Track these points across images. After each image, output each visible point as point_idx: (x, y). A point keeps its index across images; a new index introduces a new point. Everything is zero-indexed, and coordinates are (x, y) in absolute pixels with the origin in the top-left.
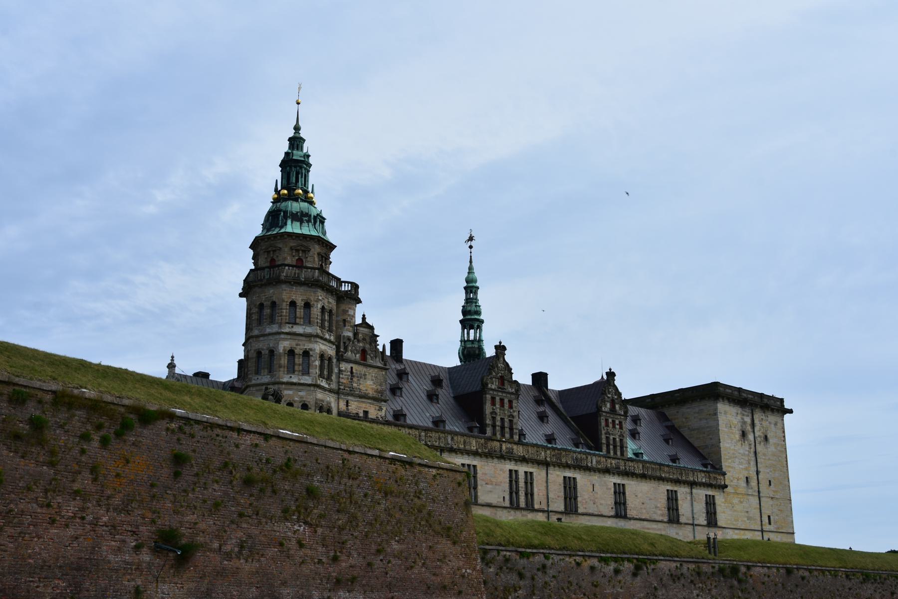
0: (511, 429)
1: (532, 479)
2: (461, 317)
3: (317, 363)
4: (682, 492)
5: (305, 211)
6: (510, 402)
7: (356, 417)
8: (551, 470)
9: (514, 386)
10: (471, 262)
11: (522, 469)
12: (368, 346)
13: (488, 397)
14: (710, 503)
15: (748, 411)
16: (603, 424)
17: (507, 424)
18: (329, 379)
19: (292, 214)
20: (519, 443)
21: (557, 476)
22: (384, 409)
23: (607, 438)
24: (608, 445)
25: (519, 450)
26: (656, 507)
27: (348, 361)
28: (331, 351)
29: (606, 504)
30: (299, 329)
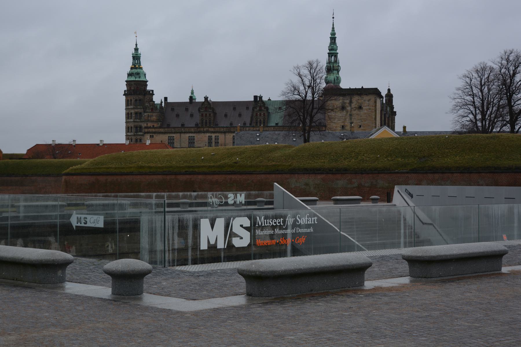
6: (210, 114)
7: (150, 128)
8: (227, 134)
10: (333, 25)
11: (213, 135)
18: (140, 119)
20: (213, 127)
23: (257, 120)
24: (257, 123)
25: (212, 130)
27: (147, 112)
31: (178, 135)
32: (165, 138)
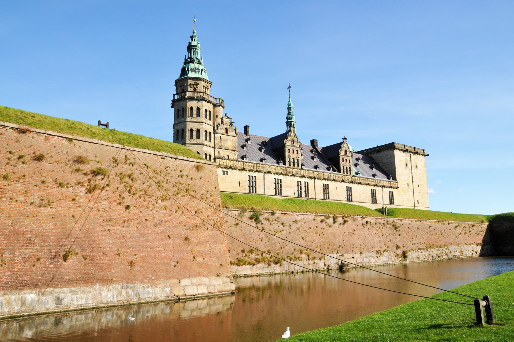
0: (298, 163)
1: (308, 185)
2: (286, 121)
3: (204, 134)
4: (378, 190)
5: (197, 67)
6: (297, 151)
7: (224, 158)
9: (299, 144)
11: (303, 180)
12: (228, 127)
13: (287, 149)
14: (391, 195)
15: (408, 154)
16: (341, 160)
17: (296, 161)
19: (191, 69)
21: (320, 183)
22: (237, 154)
24: (344, 170)
26: (366, 197)
28: (210, 129)
29: (343, 196)
30: (193, 119)
31: (261, 175)
32: (244, 176)
